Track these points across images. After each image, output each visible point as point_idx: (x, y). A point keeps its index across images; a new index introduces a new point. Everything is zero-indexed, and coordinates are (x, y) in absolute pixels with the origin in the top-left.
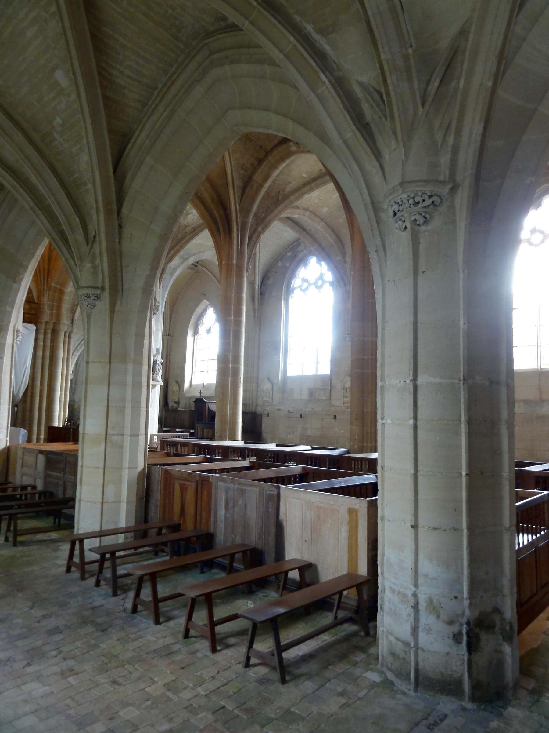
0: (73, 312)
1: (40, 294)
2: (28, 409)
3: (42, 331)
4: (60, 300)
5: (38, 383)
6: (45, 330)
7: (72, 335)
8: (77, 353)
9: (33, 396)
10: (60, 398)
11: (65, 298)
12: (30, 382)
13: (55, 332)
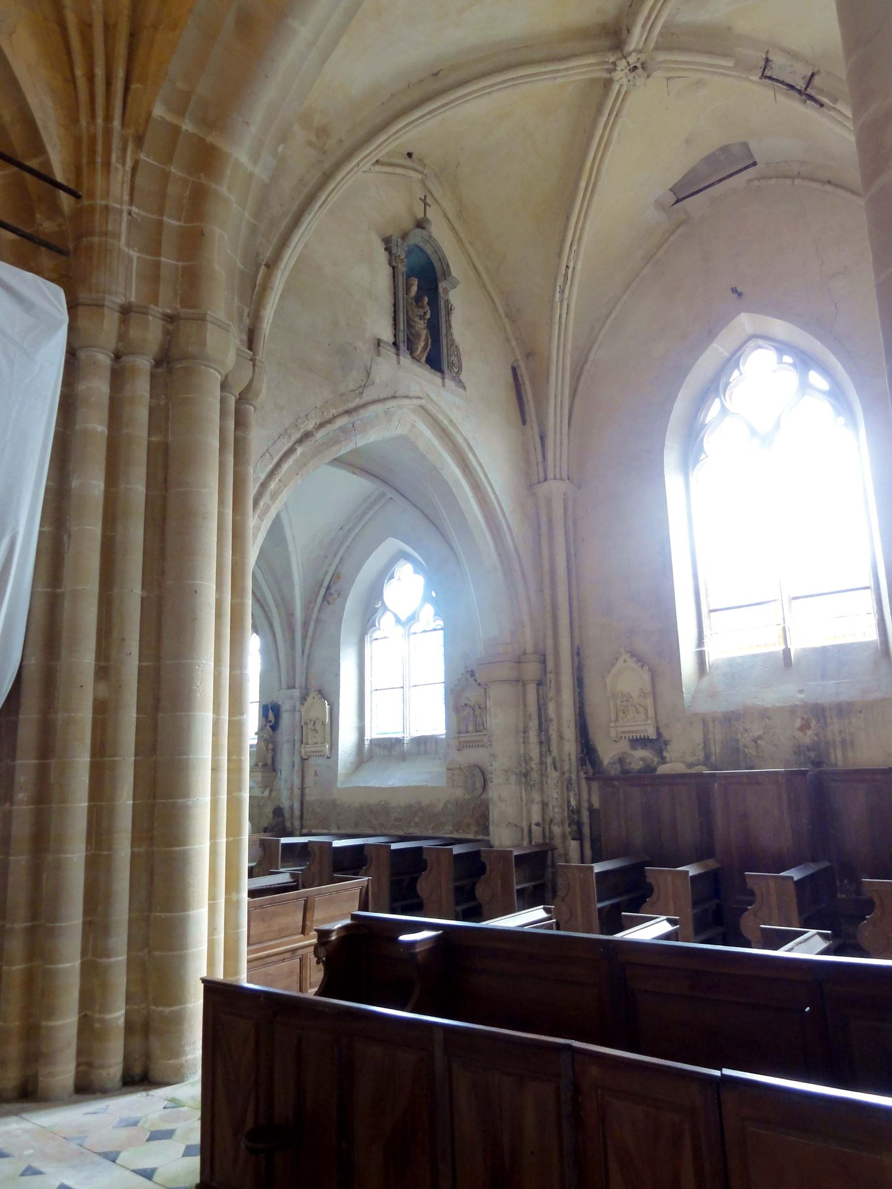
1: (87, 153)
3: (104, 359)
4: (198, 203)
6: (117, 357)
7: (253, 416)
12: (33, 661)
13: (173, 366)
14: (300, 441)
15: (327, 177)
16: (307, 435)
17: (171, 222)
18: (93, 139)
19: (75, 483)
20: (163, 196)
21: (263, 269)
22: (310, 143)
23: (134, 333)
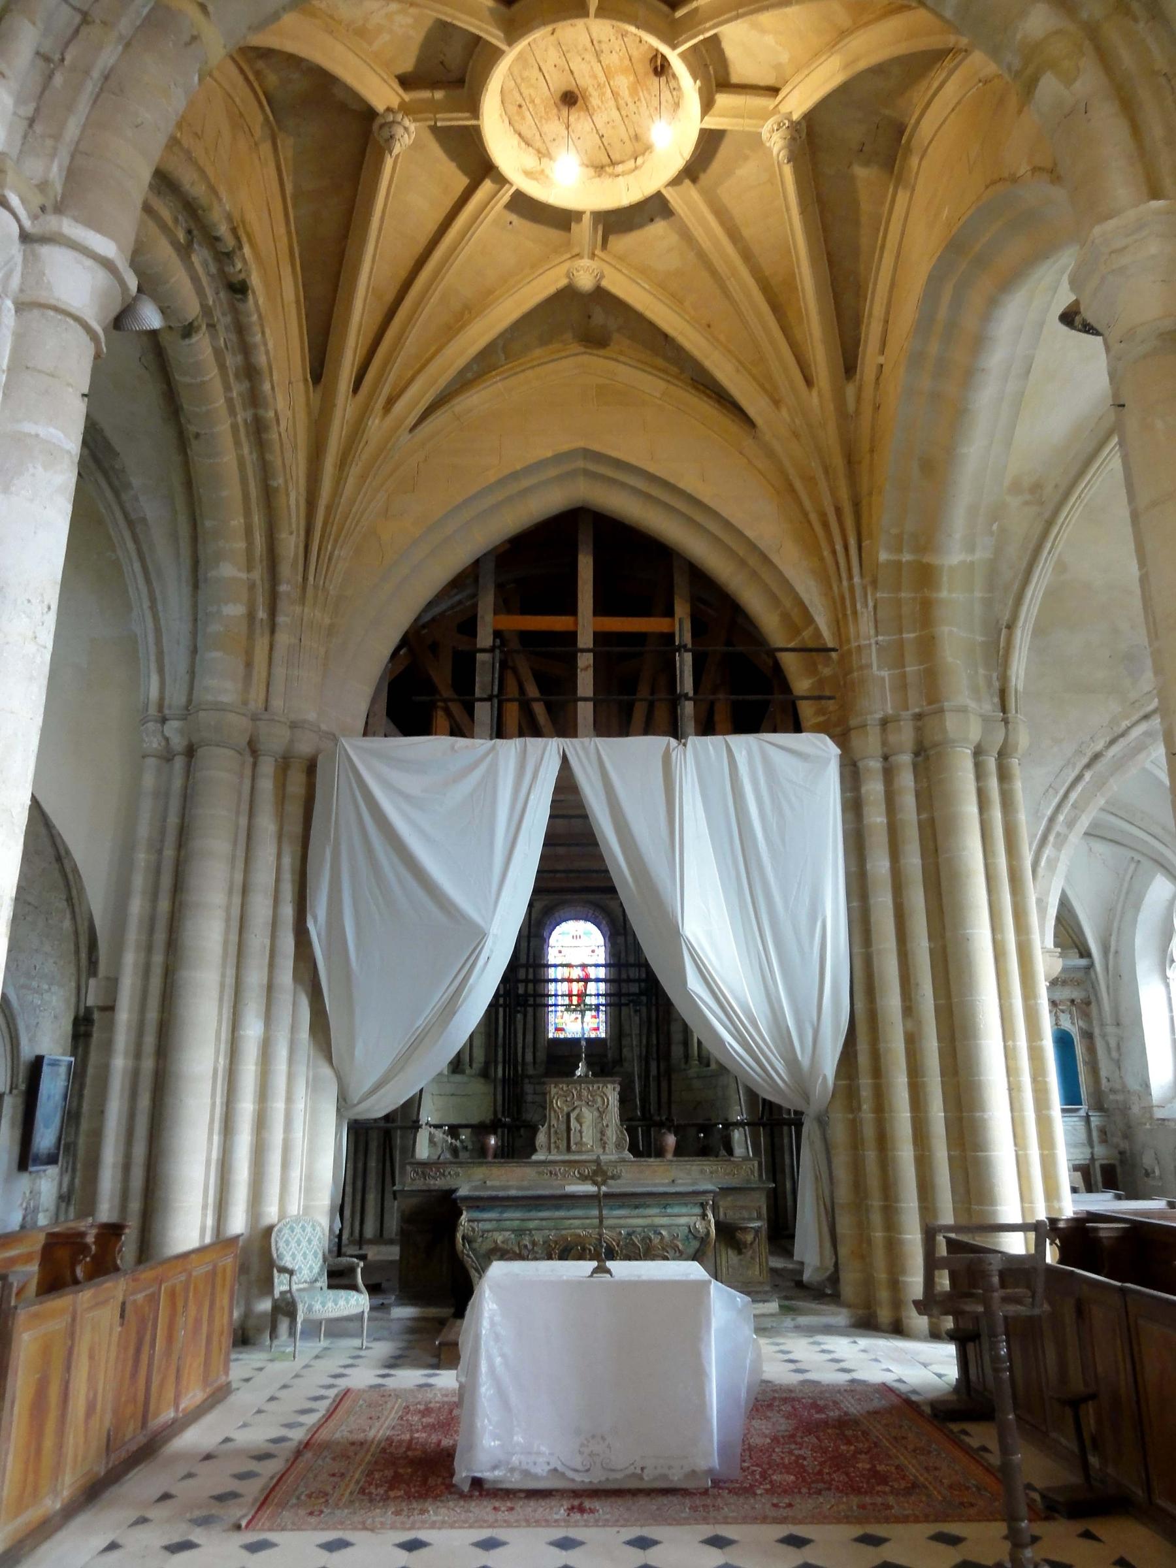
0: (997, 653)
2: (869, 1132)
3: (875, 765)
4: (926, 614)
5: (892, 1001)
6: (886, 758)
8: (1059, 846)
9: (878, 1071)
10: (1011, 1071)
11: (944, 594)
12: (859, 1006)
14: (1088, 766)
15: (1049, 524)
16: (1097, 757)
17: (909, 636)
18: (843, 598)
19: (869, 866)
20: (900, 617)
21: (1004, 631)
22: (1026, 503)
23: (892, 738)
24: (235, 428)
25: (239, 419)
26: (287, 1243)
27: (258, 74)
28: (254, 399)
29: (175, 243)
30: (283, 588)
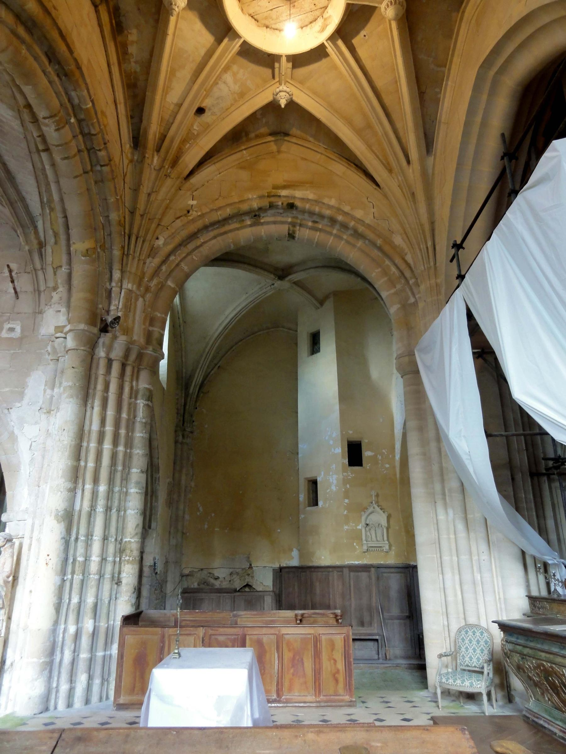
24: (348, 242)
25: (345, 237)
26: (463, 640)
27: (257, 137)
28: (344, 226)
29: (251, 226)
30: (411, 282)
